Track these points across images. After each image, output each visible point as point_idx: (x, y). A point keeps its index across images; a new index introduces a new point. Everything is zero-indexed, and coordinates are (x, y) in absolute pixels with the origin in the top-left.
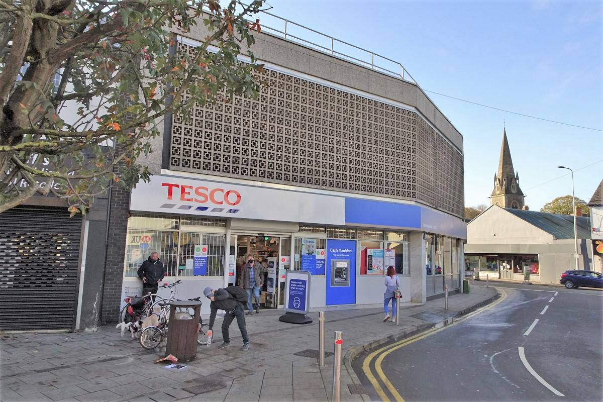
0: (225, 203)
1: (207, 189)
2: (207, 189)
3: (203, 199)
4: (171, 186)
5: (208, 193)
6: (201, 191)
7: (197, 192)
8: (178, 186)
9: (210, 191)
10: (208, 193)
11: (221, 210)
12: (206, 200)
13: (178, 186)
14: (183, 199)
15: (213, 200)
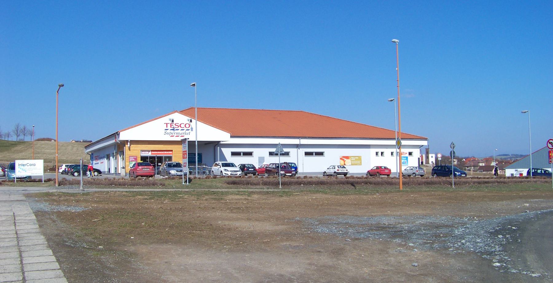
0: (185, 127)
1: (178, 124)
2: (178, 124)
3: (177, 127)
4: (167, 124)
5: (179, 125)
6: (176, 124)
7: (175, 125)
8: (169, 124)
9: (179, 124)
10: (179, 125)
11: (183, 130)
12: (178, 127)
13: (169, 124)
14: (171, 127)
15: (180, 127)
